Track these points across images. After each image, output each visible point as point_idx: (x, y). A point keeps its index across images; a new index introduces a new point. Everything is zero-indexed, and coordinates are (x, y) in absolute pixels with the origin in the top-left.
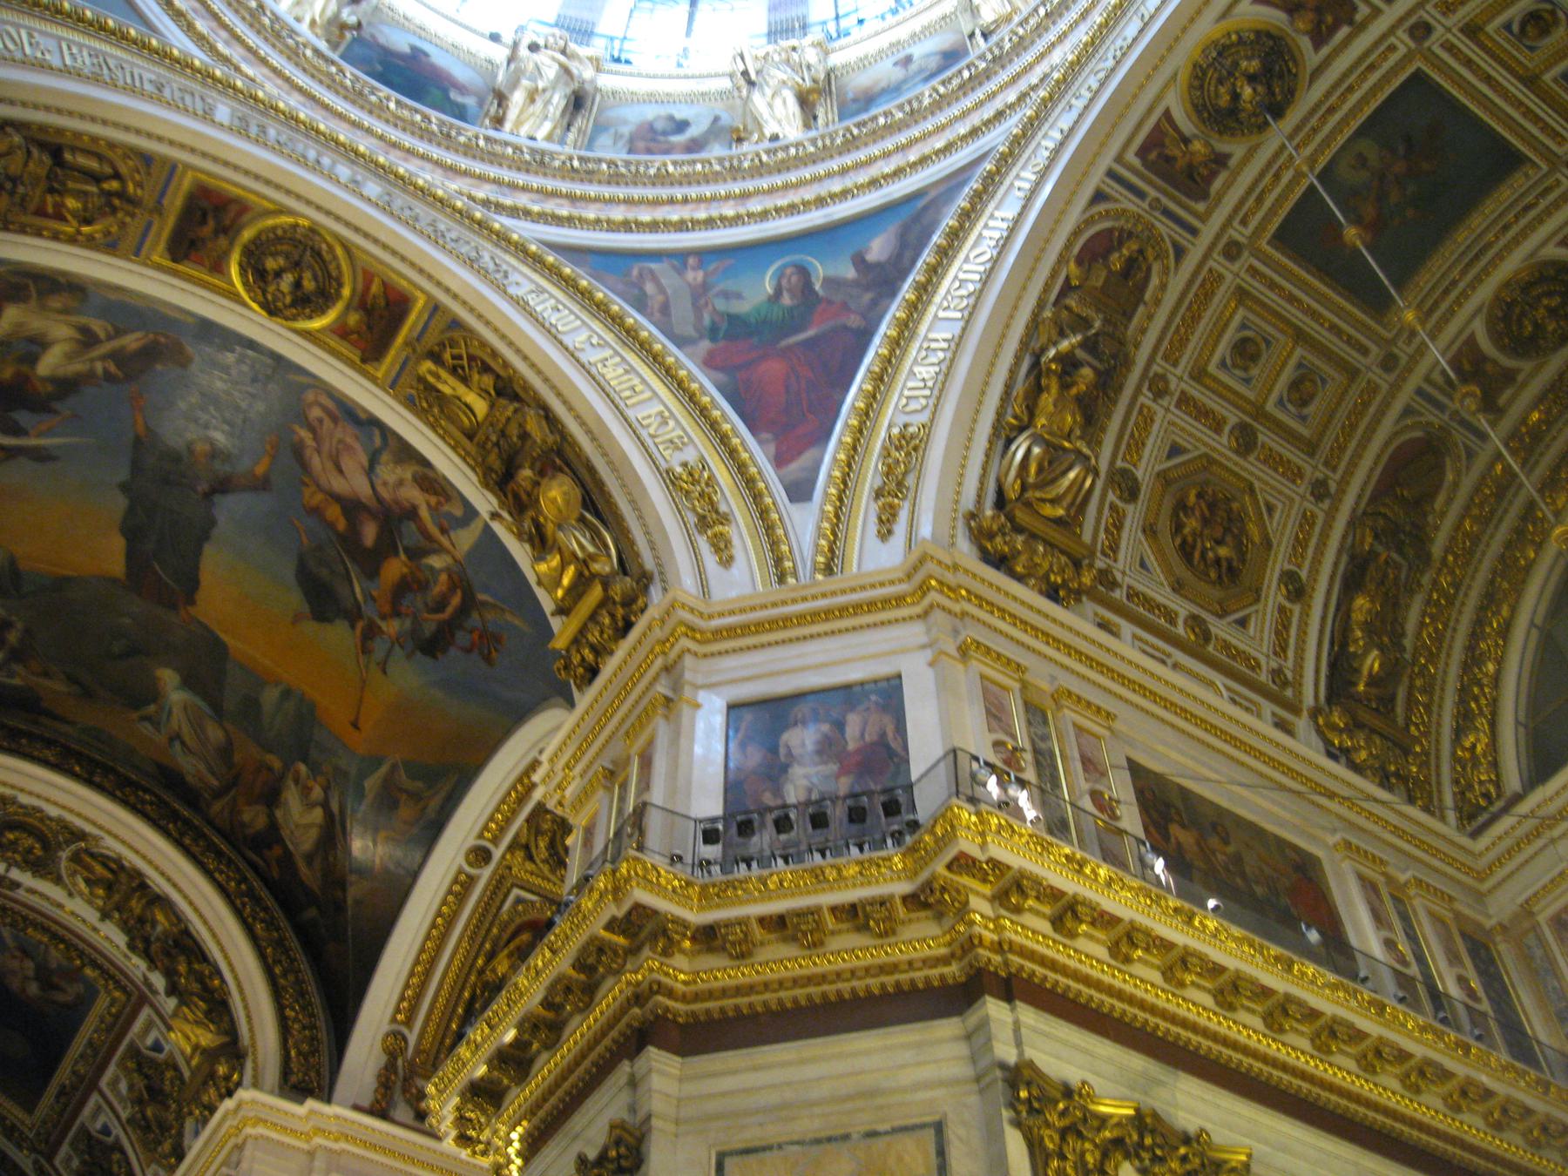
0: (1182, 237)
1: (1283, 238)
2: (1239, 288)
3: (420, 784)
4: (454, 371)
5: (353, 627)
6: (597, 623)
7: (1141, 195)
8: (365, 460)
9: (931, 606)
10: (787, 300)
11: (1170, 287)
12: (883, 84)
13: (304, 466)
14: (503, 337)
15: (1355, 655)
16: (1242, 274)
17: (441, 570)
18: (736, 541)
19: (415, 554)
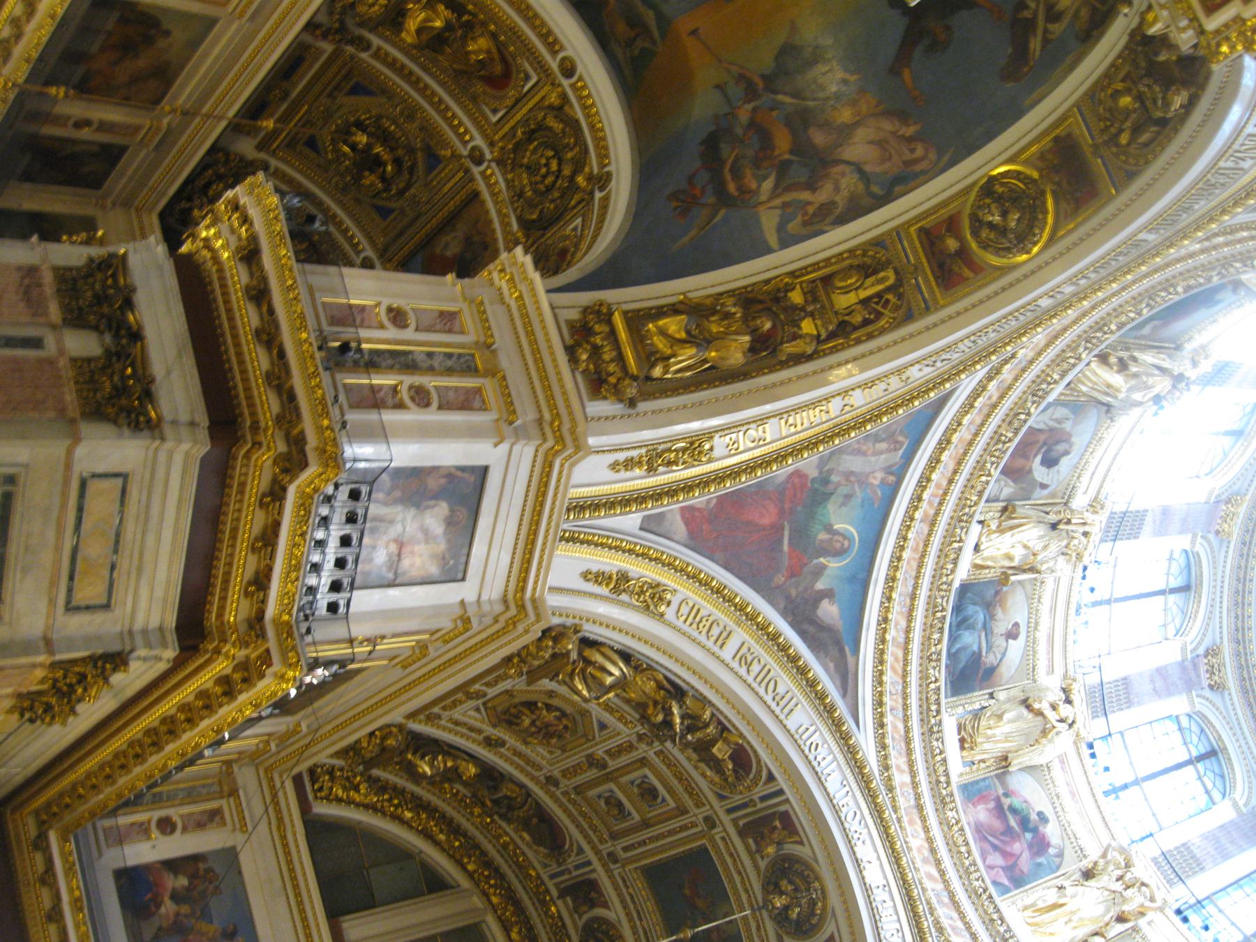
0: (730, 804)
1: (703, 851)
2: (687, 812)
3: (636, 52)
4: (879, 295)
5: (763, 76)
6: (612, 361)
7: (763, 799)
8: (868, 168)
9: (507, 608)
10: (823, 536)
11: (703, 779)
12: (999, 613)
13: (887, 114)
14: (880, 349)
15: (434, 758)
16: (694, 819)
17: (759, 186)
18: (629, 474)
19: (783, 169)
